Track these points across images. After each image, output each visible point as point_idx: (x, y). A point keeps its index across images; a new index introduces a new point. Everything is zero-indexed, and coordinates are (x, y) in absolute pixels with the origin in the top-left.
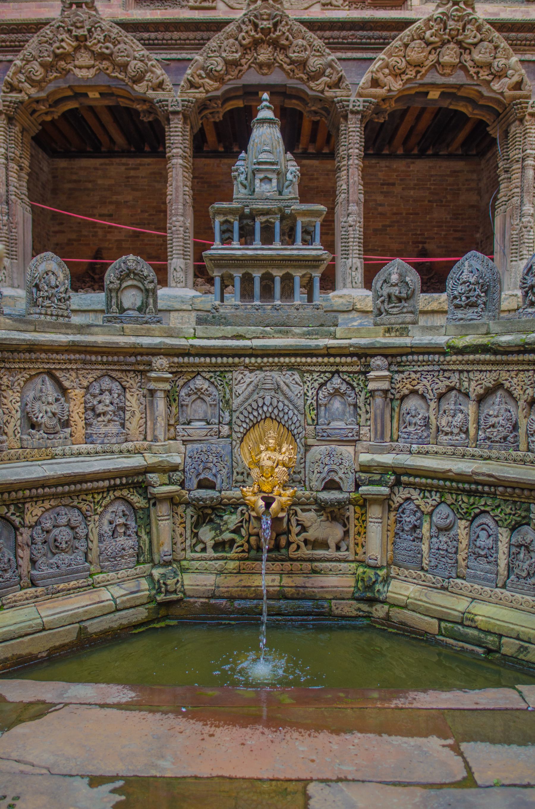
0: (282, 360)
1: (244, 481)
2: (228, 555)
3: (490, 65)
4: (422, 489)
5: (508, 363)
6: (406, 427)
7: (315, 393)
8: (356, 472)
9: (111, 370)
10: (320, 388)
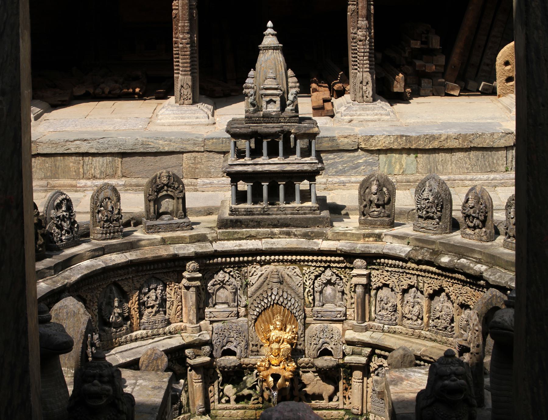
0: (286, 257)
1: (258, 351)
2: (247, 405)
5: (446, 276)
6: (380, 311)
7: (312, 283)
9: (156, 273)
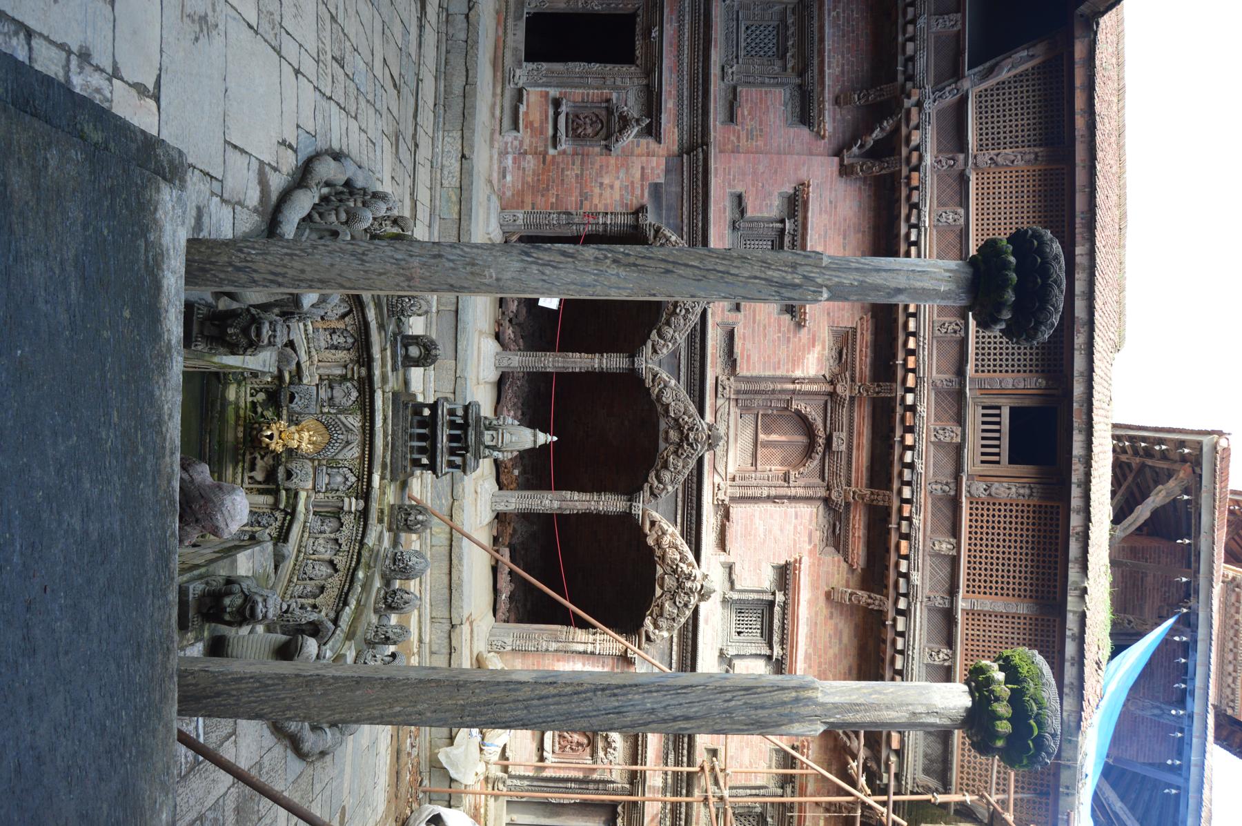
3: (661, 615)
4: (281, 527)
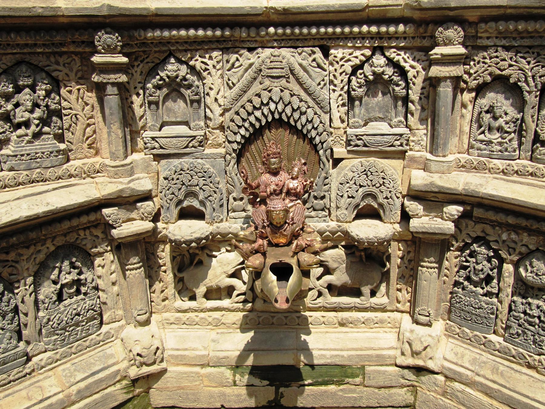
6: (483, 132)
7: (346, 80)
8: (403, 197)
10: (354, 73)
